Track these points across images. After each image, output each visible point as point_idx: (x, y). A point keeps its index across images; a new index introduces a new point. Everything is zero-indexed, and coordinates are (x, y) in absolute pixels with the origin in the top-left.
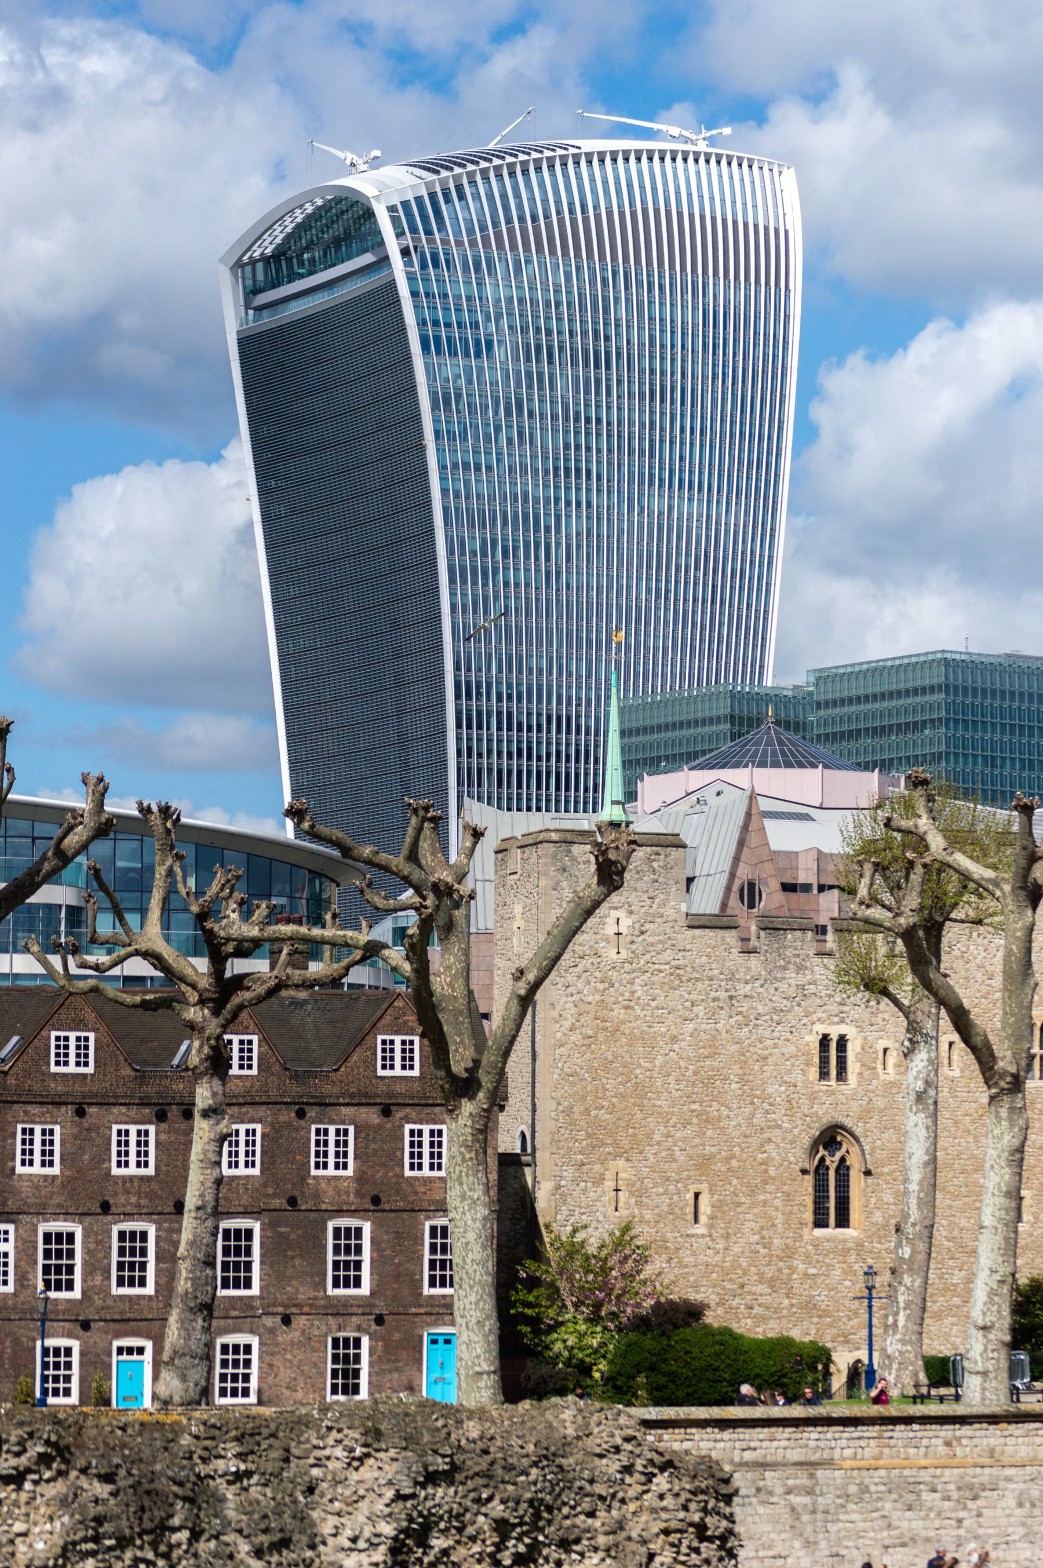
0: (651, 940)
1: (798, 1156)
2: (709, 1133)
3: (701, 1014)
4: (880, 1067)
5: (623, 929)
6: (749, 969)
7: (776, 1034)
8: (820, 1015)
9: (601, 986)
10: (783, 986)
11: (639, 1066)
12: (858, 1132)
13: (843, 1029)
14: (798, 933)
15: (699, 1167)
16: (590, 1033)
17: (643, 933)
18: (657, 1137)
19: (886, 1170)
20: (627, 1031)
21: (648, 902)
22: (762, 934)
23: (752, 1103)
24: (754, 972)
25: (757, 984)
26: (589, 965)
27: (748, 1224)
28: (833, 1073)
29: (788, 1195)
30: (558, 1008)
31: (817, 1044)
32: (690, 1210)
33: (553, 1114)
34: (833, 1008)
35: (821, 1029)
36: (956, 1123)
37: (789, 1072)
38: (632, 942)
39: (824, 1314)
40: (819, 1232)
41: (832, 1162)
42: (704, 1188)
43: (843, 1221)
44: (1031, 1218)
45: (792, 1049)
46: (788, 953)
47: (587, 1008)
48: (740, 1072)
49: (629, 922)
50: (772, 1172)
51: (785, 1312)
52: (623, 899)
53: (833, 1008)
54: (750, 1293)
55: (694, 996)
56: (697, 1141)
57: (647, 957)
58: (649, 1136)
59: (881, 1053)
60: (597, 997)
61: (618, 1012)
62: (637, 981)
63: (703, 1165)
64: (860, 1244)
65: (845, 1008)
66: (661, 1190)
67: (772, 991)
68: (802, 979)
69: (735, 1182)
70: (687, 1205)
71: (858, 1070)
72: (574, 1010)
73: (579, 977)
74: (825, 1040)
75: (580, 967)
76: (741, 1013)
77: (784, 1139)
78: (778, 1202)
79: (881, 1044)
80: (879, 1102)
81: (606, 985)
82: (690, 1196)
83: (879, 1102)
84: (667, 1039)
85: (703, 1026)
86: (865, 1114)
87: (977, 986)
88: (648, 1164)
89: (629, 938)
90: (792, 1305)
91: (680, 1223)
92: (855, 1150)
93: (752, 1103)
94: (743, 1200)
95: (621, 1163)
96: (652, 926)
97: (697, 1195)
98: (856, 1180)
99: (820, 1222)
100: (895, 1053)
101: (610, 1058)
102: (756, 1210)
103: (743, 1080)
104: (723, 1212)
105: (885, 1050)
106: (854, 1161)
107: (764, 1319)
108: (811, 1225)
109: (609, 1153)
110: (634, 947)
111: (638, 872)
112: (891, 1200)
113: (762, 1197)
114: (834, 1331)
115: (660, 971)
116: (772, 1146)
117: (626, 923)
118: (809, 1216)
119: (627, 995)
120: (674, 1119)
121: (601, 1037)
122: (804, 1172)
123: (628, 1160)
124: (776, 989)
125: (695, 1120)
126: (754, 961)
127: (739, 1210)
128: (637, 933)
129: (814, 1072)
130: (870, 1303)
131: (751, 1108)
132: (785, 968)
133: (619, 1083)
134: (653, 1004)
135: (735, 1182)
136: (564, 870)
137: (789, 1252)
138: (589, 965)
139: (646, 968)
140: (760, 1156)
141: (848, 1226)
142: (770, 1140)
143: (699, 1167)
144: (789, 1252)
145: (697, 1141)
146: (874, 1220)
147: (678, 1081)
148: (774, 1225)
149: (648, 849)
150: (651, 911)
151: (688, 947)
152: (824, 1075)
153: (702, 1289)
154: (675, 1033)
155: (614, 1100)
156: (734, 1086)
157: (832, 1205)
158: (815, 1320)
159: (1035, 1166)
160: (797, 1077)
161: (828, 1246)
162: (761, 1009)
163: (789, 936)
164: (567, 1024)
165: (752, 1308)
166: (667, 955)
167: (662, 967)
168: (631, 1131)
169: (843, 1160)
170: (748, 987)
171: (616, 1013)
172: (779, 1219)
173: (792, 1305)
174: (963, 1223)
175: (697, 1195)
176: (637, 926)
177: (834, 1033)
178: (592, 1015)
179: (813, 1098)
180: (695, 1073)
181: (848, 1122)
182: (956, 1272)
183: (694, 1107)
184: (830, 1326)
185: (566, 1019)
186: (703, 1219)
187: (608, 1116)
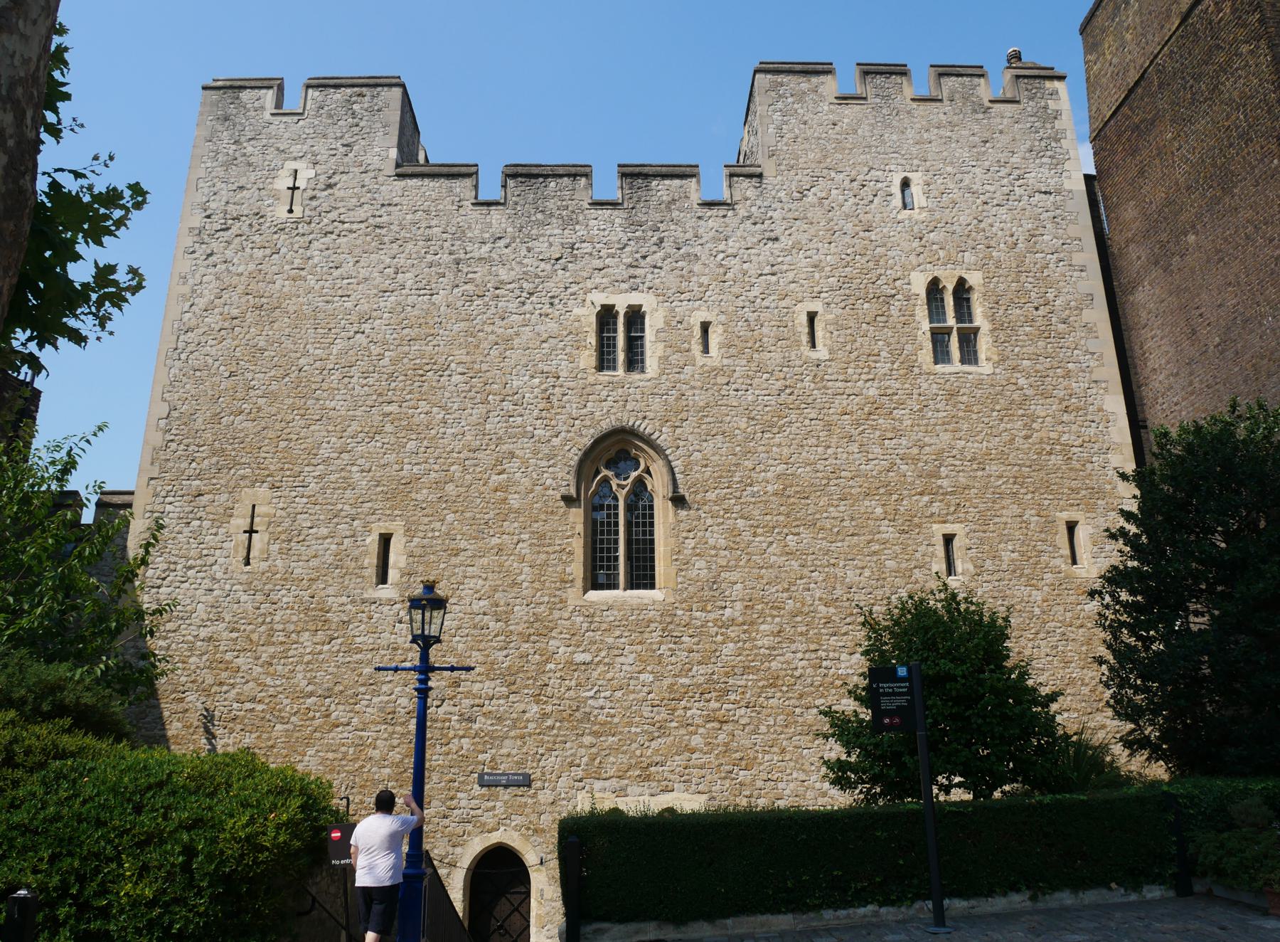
0: (342, 194)
1: (562, 478)
2: (411, 445)
3: (409, 283)
4: (697, 348)
5: (301, 183)
6: (490, 225)
7: (528, 307)
8: (598, 280)
9: (259, 254)
10: (540, 246)
11: (306, 354)
12: (663, 439)
13: (635, 298)
15: (390, 496)
16: (235, 312)
17: (330, 186)
18: (324, 452)
19: (711, 496)
20: (291, 309)
21: (342, 150)
22: (511, 183)
23: (485, 402)
24: (496, 229)
25: (502, 243)
27: (471, 583)
29: (542, 536)
30: (191, 282)
31: (593, 319)
32: (371, 560)
33: (162, 423)
34: (621, 272)
35: (600, 299)
36: (829, 426)
37: (547, 358)
39: (606, 729)
40: (594, 595)
41: (621, 489)
42: (397, 528)
43: (642, 576)
44: (971, 567)
45: (552, 326)
46: (551, 204)
47: (235, 280)
48: (465, 359)
49: (312, 173)
50: (515, 501)
51: (532, 726)
52: (305, 148)
53: (621, 272)
54: (469, 694)
55: (401, 260)
56: (391, 458)
57: (334, 215)
58: (312, 452)
59: (697, 332)
60: (252, 267)
61: (281, 285)
62: (316, 245)
63: (399, 493)
64: (667, 613)
65: (638, 272)
66: (324, 531)
67: (524, 252)
68: (569, 237)
69: (450, 517)
70: (366, 553)
71: (660, 353)
74: (606, 316)
75: (234, 230)
76: (471, 281)
77: (535, 453)
78: (524, 548)
81: (268, 251)
82: (372, 541)
83: (700, 399)
84: (354, 318)
85: (410, 300)
86: (673, 417)
87: (847, 239)
88: (307, 492)
89: (310, 193)
90: (545, 716)
91: (351, 582)
92: (658, 467)
93: (485, 402)
94: (463, 544)
95: (263, 491)
96: (345, 177)
97: (385, 540)
98: (663, 514)
99: (598, 576)
100: (720, 329)
101: (262, 344)
102: (485, 561)
103: (470, 372)
104: (427, 564)
105: (705, 327)
106: (658, 485)
107: (495, 739)
108: (579, 583)
109: (243, 478)
110: (314, 203)
111: (330, 116)
112: (722, 543)
113: (495, 541)
114: (624, 759)
115: (351, 231)
116: (516, 463)
117: (306, 174)
118: (577, 569)
119: (297, 262)
120: (355, 426)
121: (250, 317)
122: (568, 500)
123: (273, 487)
124: (529, 250)
125: (389, 428)
126: (496, 215)
127: (454, 560)
128: (321, 186)
129: (588, 358)
130: (424, 681)
131: (482, 409)
132: (543, 224)
133: (274, 378)
134: (336, 273)
135: (450, 517)
136: (226, 119)
137: (541, 629)
138: (245, 228)
139: (330, 229)
140: (495, 477)
141: (652, 586)
142: (512, 455)
143: (390, 496)
144: (541, 629)
145: (391, 458)
146: (693, 573)
147: (365, 375)
148: (514, 584)
149: (349, 91)
150: (346, 160)
151: (396, 200)
152: (604, 361)
153: (385, 688)
154: (366, 307)
155: (261, 401)
156: (456, 378)
157: (618, 549)
158: (588, 740)
159: (967, 487)
161: (610, 616)
162: (504, 274)
163: (553, 184)
164: (202, 303)
165: (471, 720)
166: (361, 213)
167: (355, 226)
168: (283, 444)
169: (640, 482)
170: (486, 248)
171: (278, 285)
172: (526, 574)
173: (545, 716)
174: (851, 576)
175: (385, 540)
176: (322, 178)
177: (622, 303)
178: (240, 289)
179: (585, 394)
180: (394, 362)
181: (646, 427)
182: (844, 657)
183: (393, 408)
184: (615, 750)
185: (201, 296)
186: (393, 574)
187: (250, 424)
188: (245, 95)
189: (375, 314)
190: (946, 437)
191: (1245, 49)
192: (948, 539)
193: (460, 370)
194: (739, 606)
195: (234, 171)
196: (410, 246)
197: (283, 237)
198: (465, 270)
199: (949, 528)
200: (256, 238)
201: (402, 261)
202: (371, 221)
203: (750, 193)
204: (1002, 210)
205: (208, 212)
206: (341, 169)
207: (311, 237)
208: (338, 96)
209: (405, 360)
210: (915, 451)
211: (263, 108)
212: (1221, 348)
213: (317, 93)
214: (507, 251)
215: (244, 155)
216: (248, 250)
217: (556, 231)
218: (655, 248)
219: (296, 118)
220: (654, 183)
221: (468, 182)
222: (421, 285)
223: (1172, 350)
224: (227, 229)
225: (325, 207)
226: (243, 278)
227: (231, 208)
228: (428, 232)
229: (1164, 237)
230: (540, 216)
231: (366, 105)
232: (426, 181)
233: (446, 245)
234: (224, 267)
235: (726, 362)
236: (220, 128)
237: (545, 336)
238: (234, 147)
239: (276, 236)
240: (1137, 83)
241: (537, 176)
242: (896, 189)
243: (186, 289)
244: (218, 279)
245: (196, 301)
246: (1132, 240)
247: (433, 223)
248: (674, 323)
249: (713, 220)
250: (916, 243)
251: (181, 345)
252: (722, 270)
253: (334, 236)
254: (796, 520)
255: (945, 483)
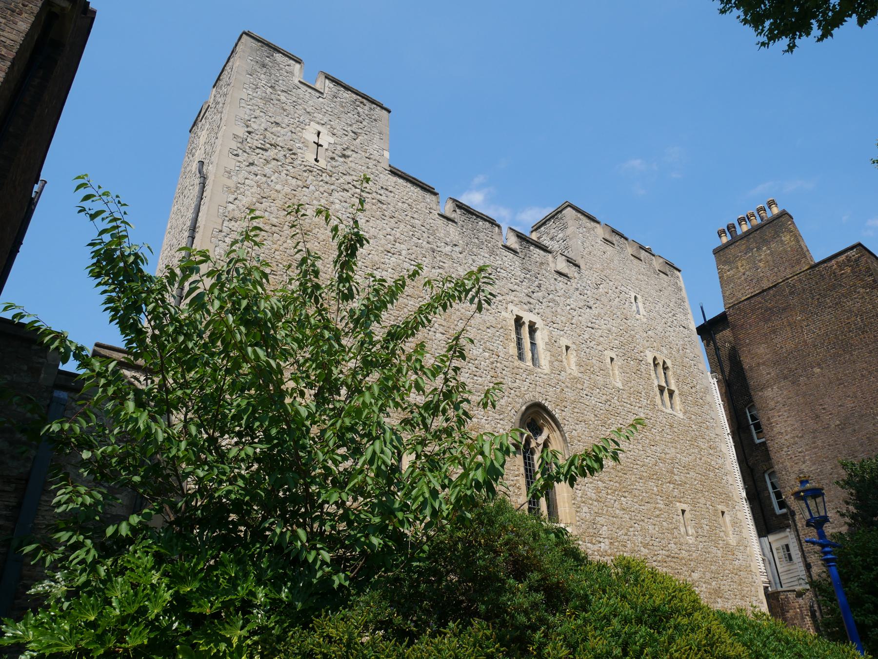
3: (404, 253)
14: (487, 224)
17: (344, 156)
25: (457, 249)
26: (280, 156)
28: (528, 355)
30: (234, 178)
38: (333, 159)
47: (274, 194)
52: (325, 119)
57: (349, 178)
60: (287, 189)
62: (335, 194)
72: (255, 189)
73: (268, 162)
79: (564, 342)
80: (570, 395)
92: (555, 437)
96: (354, 155)
126: (451, 227)
129: (513, 349)
139: (346, 187)
150: (354, 142)
151: (390, 188)
154: (376, 258)
156: (438, 335)
160: (497, 346)
176: (339, 148)
188: (278, 57)
189: (383, 266)
190: (673, 450)
191: (862, 290)
192: (683, 511)
193: (441, 330)
194: (607, 541)
195: (271, 109)
196: (402, 225)
197: (311, 177)
198: (439, 258)
199: (684, 506)
200: (290, 168)
201: (398, 235)
202: (374, 194)
203: (576, 275)
204: (671, 330)
205: (249, 129)
206: (352, 148)
207: (332, 187)
208: (348, 95)
209: (406, 310)
210: (663, 455)
211: (292, 73)
212: (842, 427)
213: (331, 85)
214: (460, 256)
215: (279, 100)
216: (283, 174)
217: (486, 255)
218: (537, 289)
219: (318, 94)
220: (531, 248)
221: (433, 198)
222: (413, 257)
223: (799, 424)
224: (266, 150)
225: (342, 169)
226: (280, 196)
227: (268, 135)
228: (412, 221)
229: (793, 366)
230: (476, 240)
231: (366, 112)
232: (409, 185)
233: (425, 235)
234: (264, 179)
235: (580, 375)
236: (259, 70)
237: (488, 324)
238: (270, 90)
239: (306, 174)
240: (770, 288)
241: (473, 214)
242: (633, 301)
243: (231, 183)
244: (258, 186)
245: (240, 197)
246: (764, 364)
247: (415, 216)
248: (552, 342)
249: (561, 284)
250: (645, 335)
251: (225, 229)
252: (570, 316)
253: (349, 194)
254: (624, 487)
255: (677, 477)
